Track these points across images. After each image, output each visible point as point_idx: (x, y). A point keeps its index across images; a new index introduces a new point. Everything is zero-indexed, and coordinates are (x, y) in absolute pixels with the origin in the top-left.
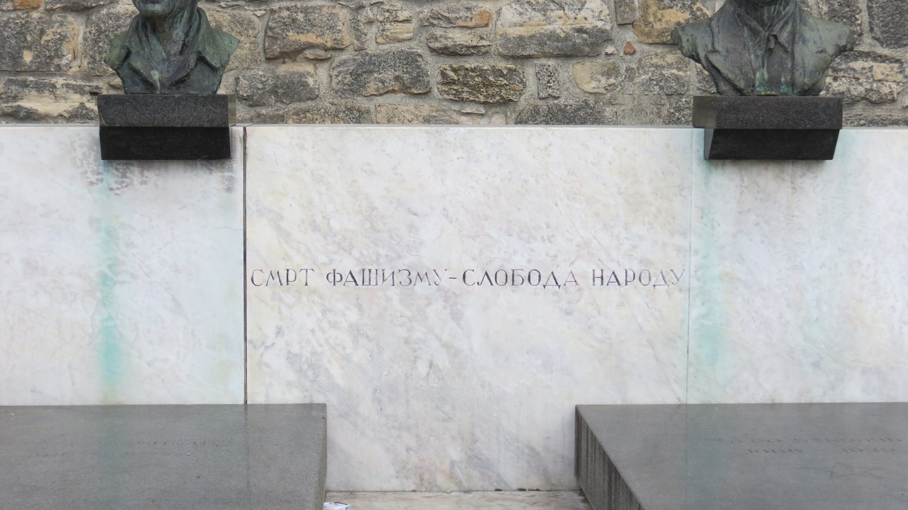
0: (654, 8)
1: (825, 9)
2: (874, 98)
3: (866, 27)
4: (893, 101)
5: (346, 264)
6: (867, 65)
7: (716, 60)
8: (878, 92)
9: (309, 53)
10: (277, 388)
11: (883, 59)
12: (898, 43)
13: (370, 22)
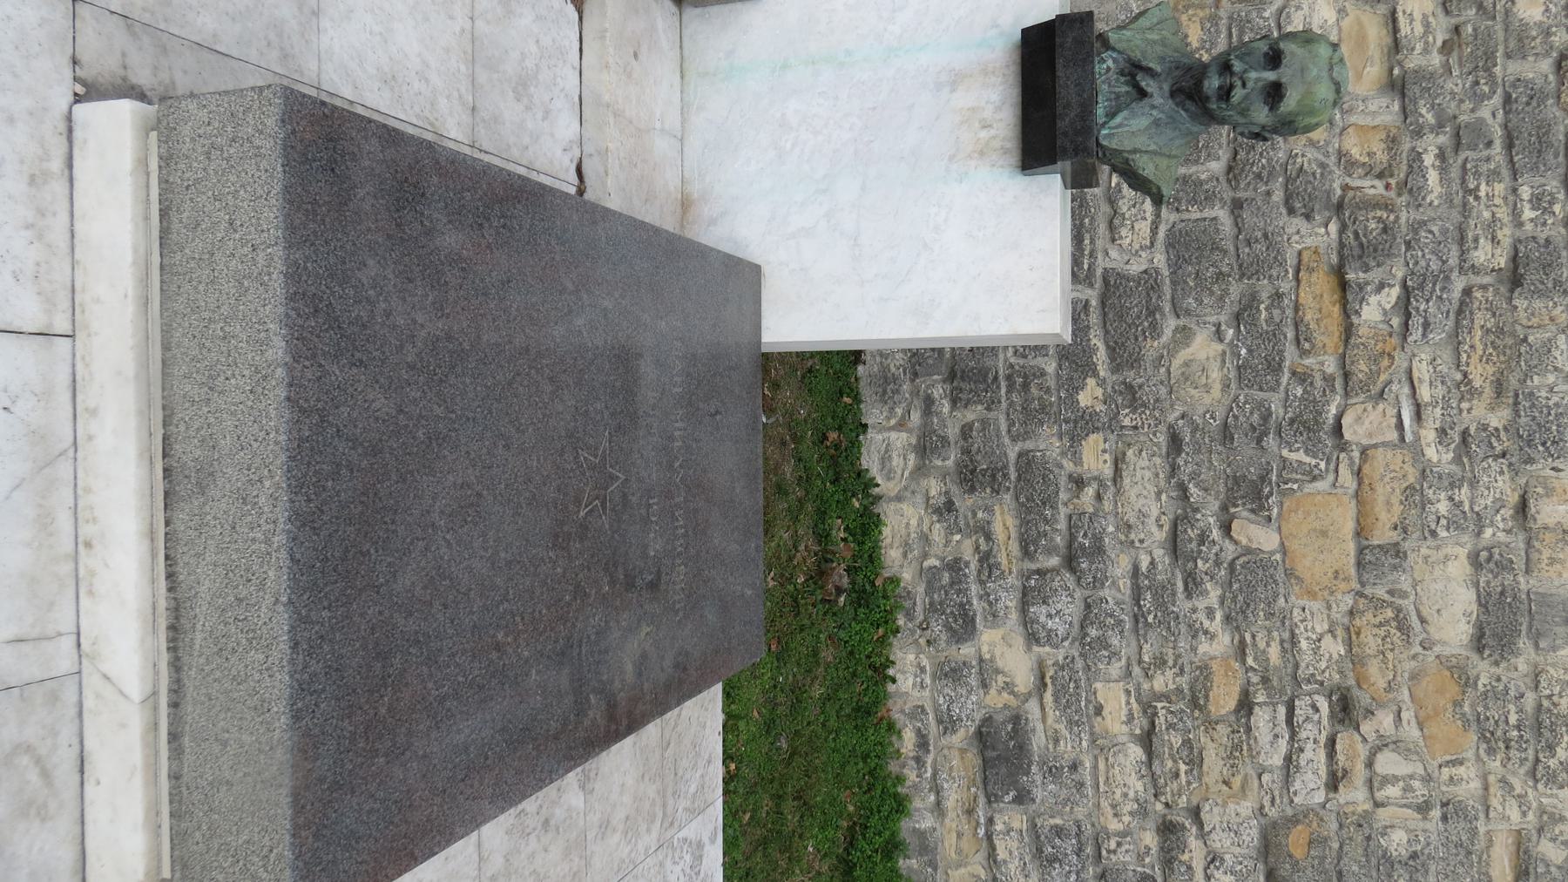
0: (1201, 14)
1: (1203, 177)
2: (1116, 222)
3: (1185, 216)
4: (1113, 240)
6: (1148, 215)
8: (1123, 225)
11: (1154, 230)
12: (1170, 245)
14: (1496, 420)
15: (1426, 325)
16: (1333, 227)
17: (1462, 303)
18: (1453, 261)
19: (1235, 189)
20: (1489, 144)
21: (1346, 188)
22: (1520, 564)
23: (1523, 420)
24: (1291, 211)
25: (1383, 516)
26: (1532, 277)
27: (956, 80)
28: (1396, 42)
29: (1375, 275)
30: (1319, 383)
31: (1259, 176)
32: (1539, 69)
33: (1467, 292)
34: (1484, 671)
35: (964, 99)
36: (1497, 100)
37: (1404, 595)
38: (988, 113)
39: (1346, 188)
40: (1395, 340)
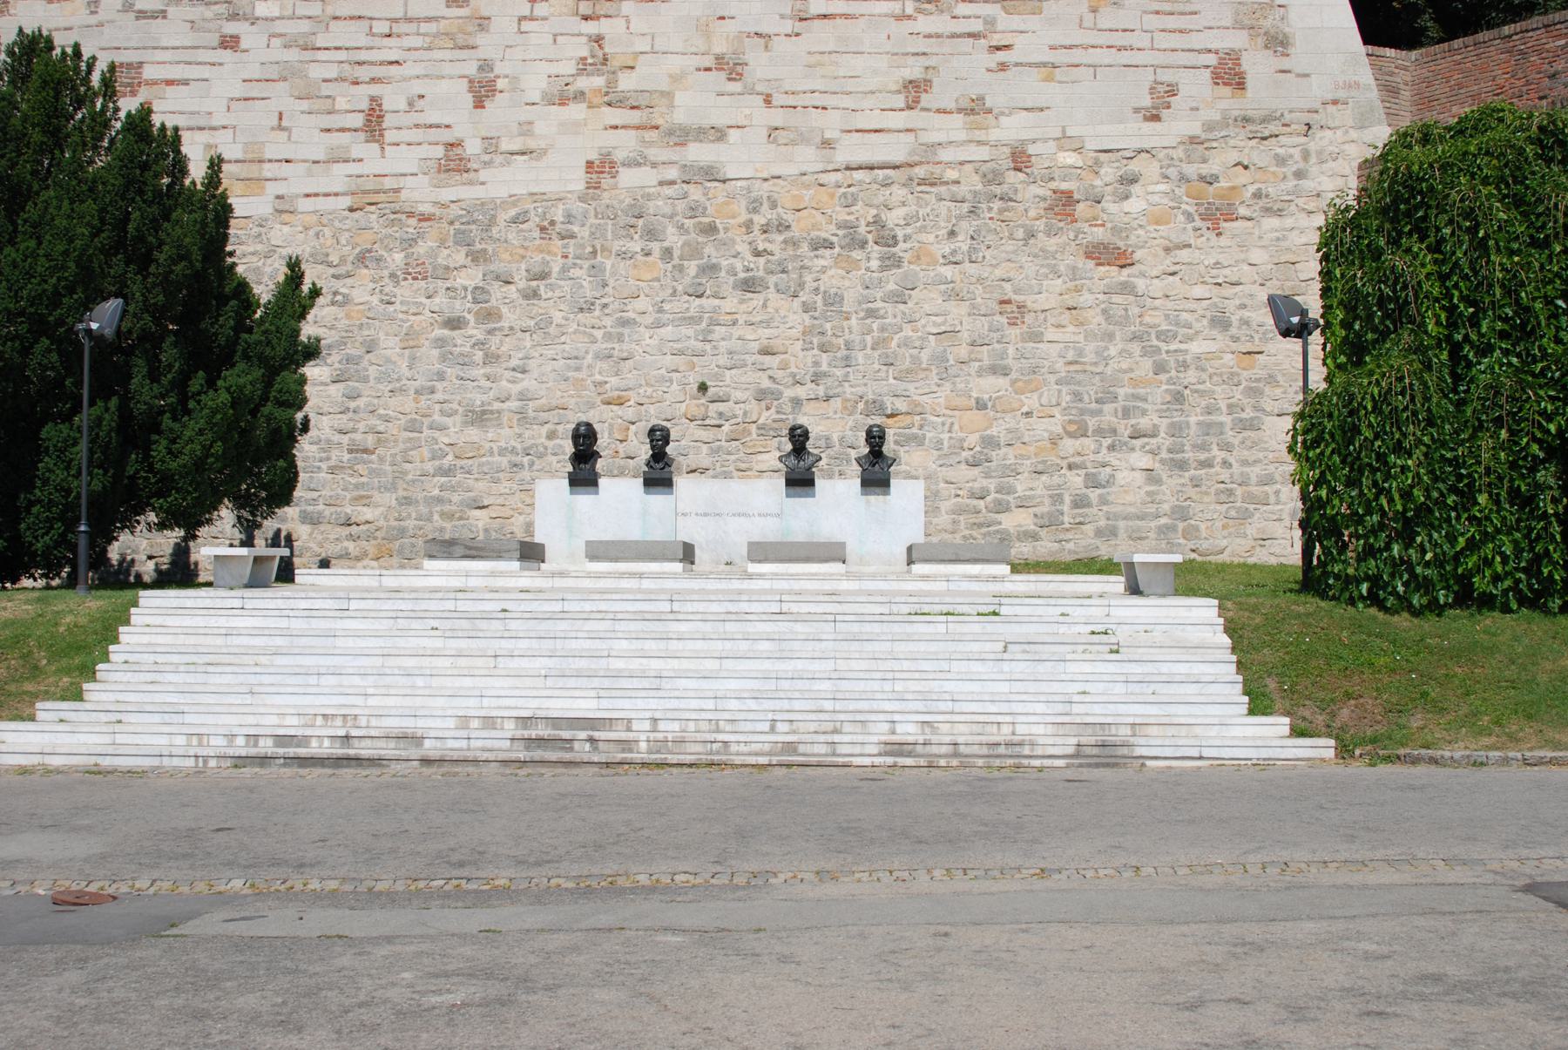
27: (868, 502)
29: (889, 405)
34: (1014, 375)
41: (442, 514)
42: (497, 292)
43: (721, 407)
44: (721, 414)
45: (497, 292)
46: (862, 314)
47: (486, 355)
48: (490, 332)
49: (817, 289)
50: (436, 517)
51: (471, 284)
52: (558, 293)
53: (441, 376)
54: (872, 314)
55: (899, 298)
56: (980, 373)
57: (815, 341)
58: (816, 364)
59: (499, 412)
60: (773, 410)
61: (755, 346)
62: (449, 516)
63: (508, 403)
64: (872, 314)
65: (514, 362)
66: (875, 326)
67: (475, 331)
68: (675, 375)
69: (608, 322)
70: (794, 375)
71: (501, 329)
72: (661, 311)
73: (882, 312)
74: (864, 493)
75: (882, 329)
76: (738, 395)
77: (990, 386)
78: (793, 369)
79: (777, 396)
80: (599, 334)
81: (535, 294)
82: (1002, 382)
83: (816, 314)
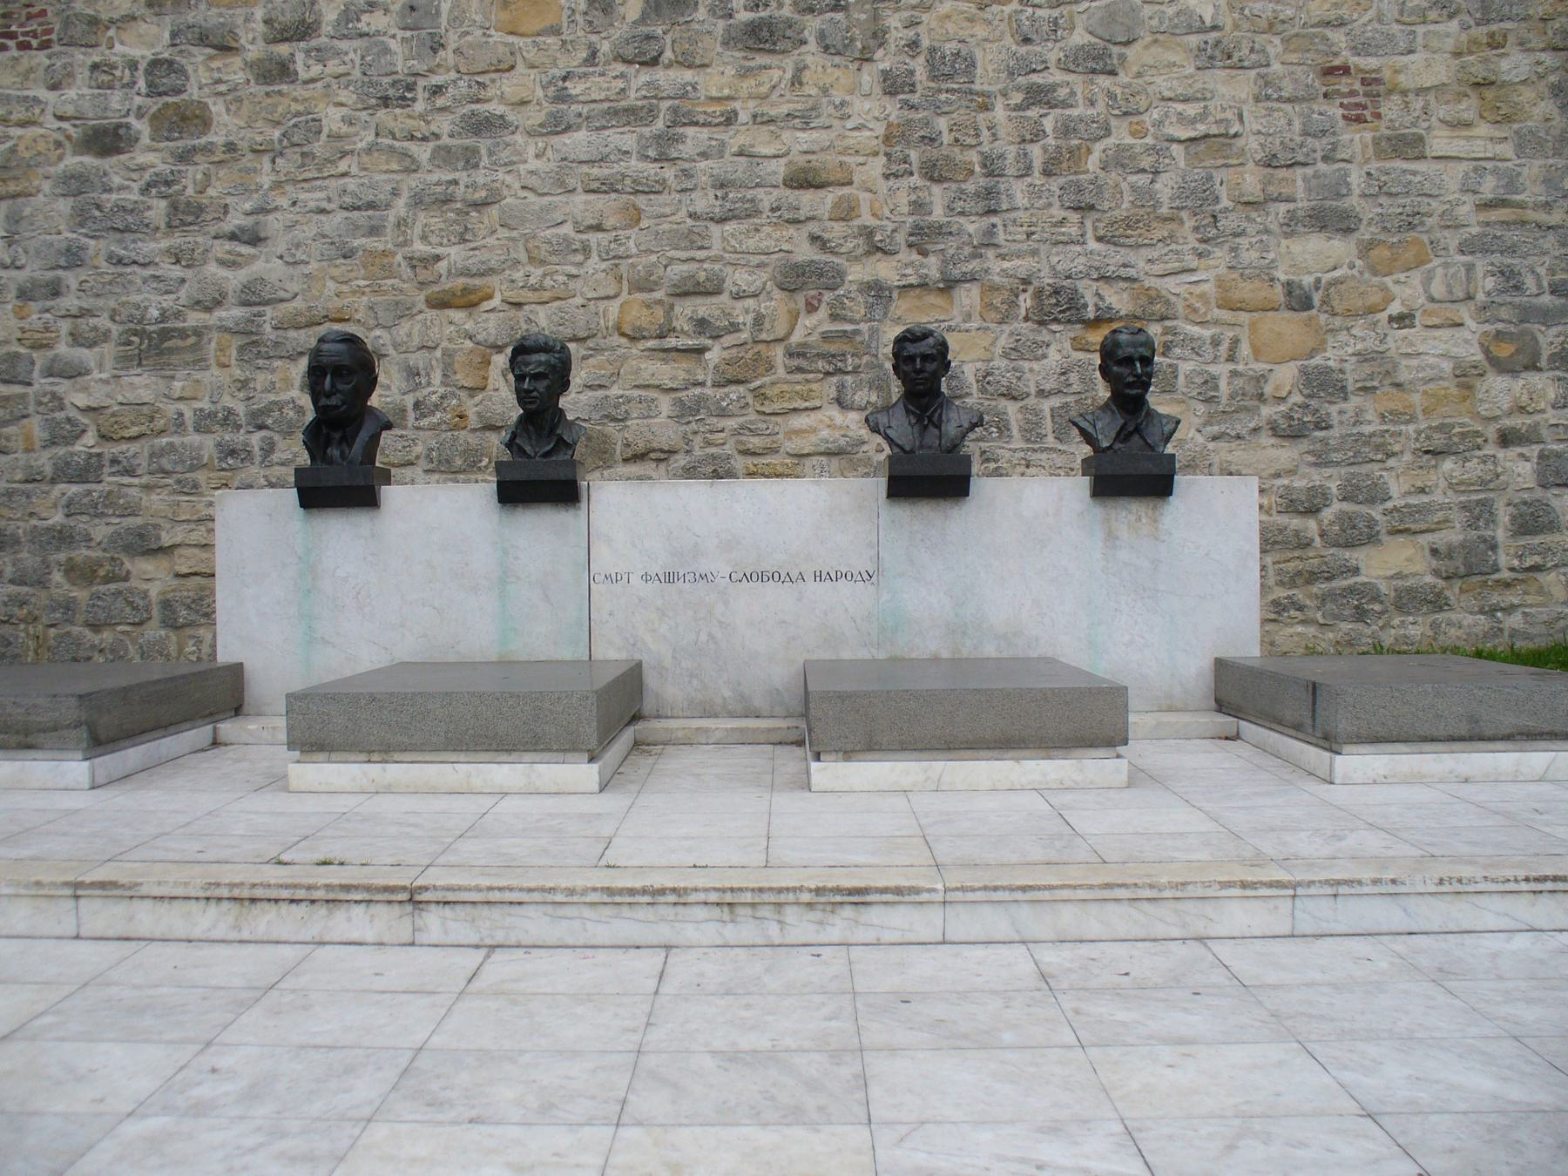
5: (655, 569)
7: (890, 432)
9: (652, 455)
10: (612, 651)
13: (696, 433)
14: (1189, 223)
15: (1125, 266)
16: (1054, 327)
17: (1108, 242)
18: (1078, 248)
19: (1028, 395)
20: (994, 226)
21: (1026, 319)
22: (1291, 206)
23: (1189, 203)
24: (1045, 356)
25: (1263, 294)
26: (1088, 199)
27: (1111, 537)
28: (920, 286)
29: (1090, 299)
30: (1170, 338)
31: (1019, 378)
32: (938, 196)
33: (1099, 239)
34: (1365, 233)
35: (1123, 532)
36: (962, 220)
37: (1318, 280)
38: (1132, 518)
39: (1026, 319)
40: (1136, 285)
41: (70, 569)
42: (200, 69)
43: (703, 307)
44: (702, 325)
45: (200, 69)
46: (1017, 98)
47: (174, 207)
48: (184, 157)
49: (914, 44)
50: (57, 577)
51: (143, 53)
52: (334, 67)
53: (74, 258)
54: (1039, 96)
55: (1096, 62)
56: (1291, 226)
57: (914, 155)
58: (918, 206)
59: (198, 332)
60: (823, 312)
61: (779, 169)
62: (81, 573)
63: (220, 313)
64: (1039, 96)
65: (234, 221)
66: (1048, 124)
67: (150, 156)
68: (593, 238)
69: (443, 124)
70: (868, 233)
71: (208, 149)
72: (562, 97)
73: (1062, 93)
74: (1097, 511)
75: (1066, 130)
76: (740, 278)
77: (1314, 256)
78: (867, 219)
79: (828, 278)
80: (423, 152)
81: (281, 71)
82: (1339, 248)
83: (915, 99)
